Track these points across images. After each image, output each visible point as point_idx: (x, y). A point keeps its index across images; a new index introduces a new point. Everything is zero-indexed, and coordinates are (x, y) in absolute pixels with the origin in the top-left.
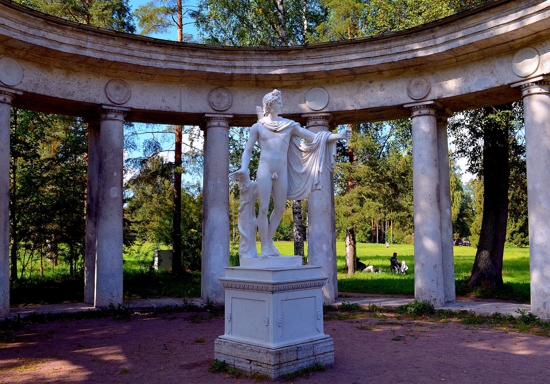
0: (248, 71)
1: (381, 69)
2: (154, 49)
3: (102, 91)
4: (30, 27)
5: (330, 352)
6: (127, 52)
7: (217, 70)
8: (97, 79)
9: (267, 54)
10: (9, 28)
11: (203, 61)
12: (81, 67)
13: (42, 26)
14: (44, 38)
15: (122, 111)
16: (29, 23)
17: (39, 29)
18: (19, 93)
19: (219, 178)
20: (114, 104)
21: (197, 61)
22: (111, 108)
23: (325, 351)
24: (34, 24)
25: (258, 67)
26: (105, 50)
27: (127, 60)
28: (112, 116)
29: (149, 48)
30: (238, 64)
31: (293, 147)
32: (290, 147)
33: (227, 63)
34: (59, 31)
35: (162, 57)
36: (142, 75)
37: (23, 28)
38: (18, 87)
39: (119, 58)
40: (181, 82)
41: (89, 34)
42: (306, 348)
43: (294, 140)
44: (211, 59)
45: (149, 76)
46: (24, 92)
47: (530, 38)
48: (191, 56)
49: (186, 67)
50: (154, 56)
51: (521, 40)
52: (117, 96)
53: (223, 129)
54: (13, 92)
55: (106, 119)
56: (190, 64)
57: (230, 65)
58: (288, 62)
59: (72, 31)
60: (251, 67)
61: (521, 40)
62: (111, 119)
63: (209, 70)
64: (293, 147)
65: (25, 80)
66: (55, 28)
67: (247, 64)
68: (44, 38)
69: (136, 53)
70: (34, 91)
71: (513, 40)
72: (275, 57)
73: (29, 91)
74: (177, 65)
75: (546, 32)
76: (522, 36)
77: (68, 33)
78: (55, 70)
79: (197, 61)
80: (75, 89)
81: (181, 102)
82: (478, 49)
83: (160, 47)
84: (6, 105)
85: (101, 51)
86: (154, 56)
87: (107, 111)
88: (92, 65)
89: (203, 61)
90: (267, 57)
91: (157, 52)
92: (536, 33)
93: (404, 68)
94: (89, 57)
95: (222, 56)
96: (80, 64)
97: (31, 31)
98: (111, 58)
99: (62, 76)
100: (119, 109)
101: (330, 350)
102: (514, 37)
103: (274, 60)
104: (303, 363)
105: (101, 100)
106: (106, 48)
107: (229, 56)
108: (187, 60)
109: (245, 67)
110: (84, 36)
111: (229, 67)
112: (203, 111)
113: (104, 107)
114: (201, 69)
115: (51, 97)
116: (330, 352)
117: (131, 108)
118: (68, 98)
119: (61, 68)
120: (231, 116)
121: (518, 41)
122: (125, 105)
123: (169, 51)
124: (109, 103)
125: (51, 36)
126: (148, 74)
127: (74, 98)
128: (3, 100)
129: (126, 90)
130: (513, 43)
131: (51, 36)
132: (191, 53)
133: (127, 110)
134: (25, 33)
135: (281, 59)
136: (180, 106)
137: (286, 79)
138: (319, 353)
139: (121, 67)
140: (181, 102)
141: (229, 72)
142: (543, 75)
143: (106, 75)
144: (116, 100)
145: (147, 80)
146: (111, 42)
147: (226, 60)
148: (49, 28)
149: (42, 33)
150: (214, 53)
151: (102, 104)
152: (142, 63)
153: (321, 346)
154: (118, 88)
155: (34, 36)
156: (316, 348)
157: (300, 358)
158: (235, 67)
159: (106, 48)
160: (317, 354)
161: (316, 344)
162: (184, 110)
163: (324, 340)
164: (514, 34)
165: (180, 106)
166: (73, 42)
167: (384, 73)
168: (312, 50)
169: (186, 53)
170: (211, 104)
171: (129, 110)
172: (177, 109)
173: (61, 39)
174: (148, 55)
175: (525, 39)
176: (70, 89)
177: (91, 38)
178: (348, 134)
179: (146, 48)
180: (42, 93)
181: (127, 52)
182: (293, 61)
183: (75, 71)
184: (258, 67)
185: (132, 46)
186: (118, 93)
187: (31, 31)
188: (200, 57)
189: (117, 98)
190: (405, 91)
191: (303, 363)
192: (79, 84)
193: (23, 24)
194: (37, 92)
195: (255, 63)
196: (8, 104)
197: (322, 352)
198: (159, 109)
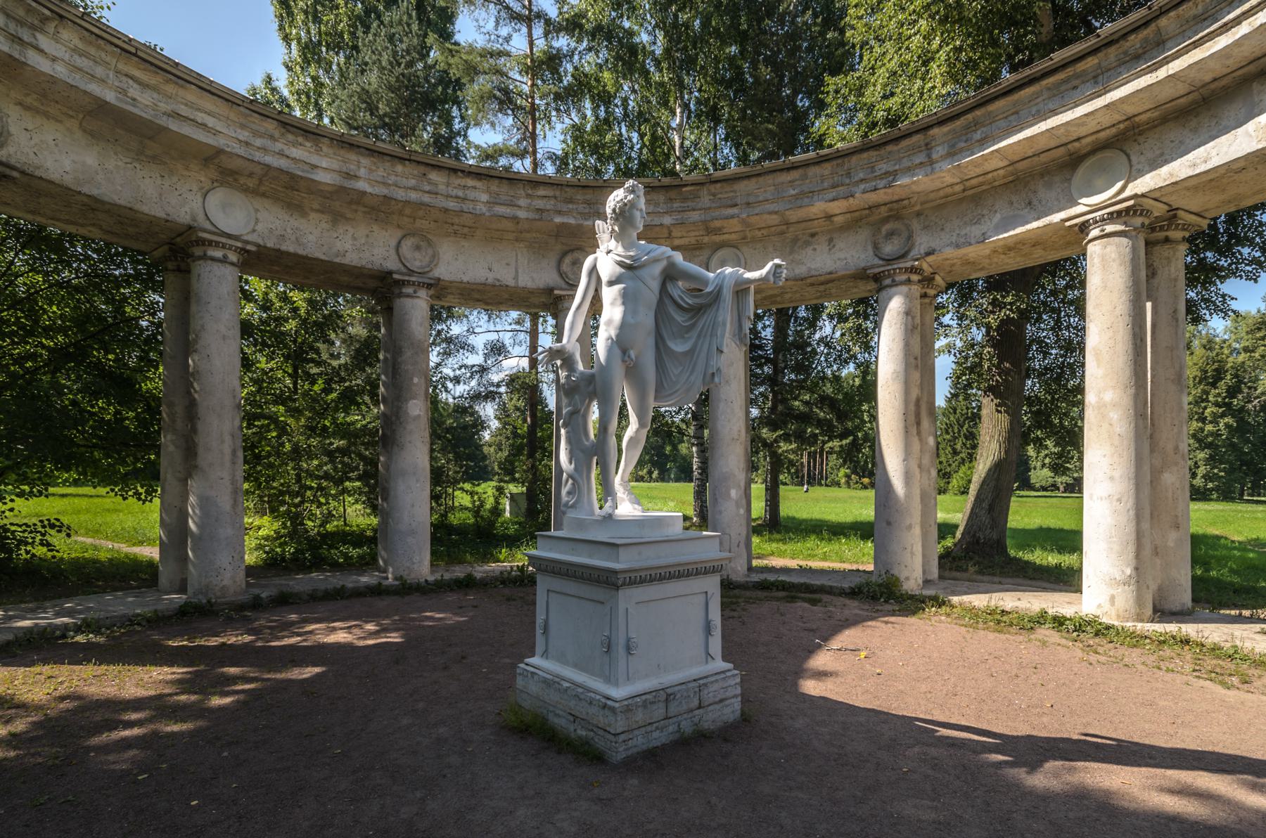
1: (832, 212)
2: (470, 182)
3: (393, 252)
4: (256, 134)
8: (384, 232)
10: (217, 133)
12: (356, 211)
14: (281, 154)
17: (272, 137)
20: (411, 272)
22: (407, 278)
27: (426, 199)
28: (410, 290)
31: (667, 301)
32: (660, 302)
34: (308, 144)
36: (456, 227)
37: (244, 135)
39: (413, 196)
40: (517, 240)
41: (362, 155)
43: (670, 288)
45: (466, 230)
46: (258, 246)
47: (1114, 130)
51: (1093, 137)
52: (417, 261)
55: (400, 295)
61: (1093, 137)
62: (408, 296)
64: (667, 301)
65: (259, 227)
66: (300, 139)
68: (281, 154)
71: (1078, 139)
75: (1149, 115)
76: (1099, 128)
77: (325, 149)
78: (313, 215)
80: (348, 246)
81: (517, 272)
82: (1006, 163)
83: (480, 180)
87: (402, 283)
88: (373, 208)
92: (1129, 119)
93: (870, 208)
94: (364, 193)
96: (354, 207)
98: (400, 194)
99: (324, 225)
102: (1083, 131)
105: (392, 264)
112: (552, 284)
113: (395, 276)
117: (439, 279)
118: (337, 260)
119: (322, 212)
121: (1089, 140)
122: (431, 275)
124: (404, 270)
125: (296, 152)
127: (346, 261)
129: (430, 252)
130: (1076, 144)
131: (296, 152)
132: (530, 192)
134: (247, 144)
136: (516, 278)
137: (679, 234)
139: (421, 213)
140: (517, 272)
142: (1135, 196)
143: (399, 226)
145: (465, 236)
146: (399, 168)
151: (390, 273)
152: (452, 205)
154: (418, 248)
155: (264, 149)
162: (521, 284)
164: (1083, 124)
165: (516, 278)
167: (835, 219)
168: (719, 185)
173: (314, 159)
174: (460, 194)
175: (1102, 135)
176: (339, 245)
179: (459, 181)
181: (427, 188)
182: (690, 204)
183: (347, 219)
186: (417, 255)
189: (417, 263)
190: (870, 248)
192: (354, 239)
193: (243, 127)
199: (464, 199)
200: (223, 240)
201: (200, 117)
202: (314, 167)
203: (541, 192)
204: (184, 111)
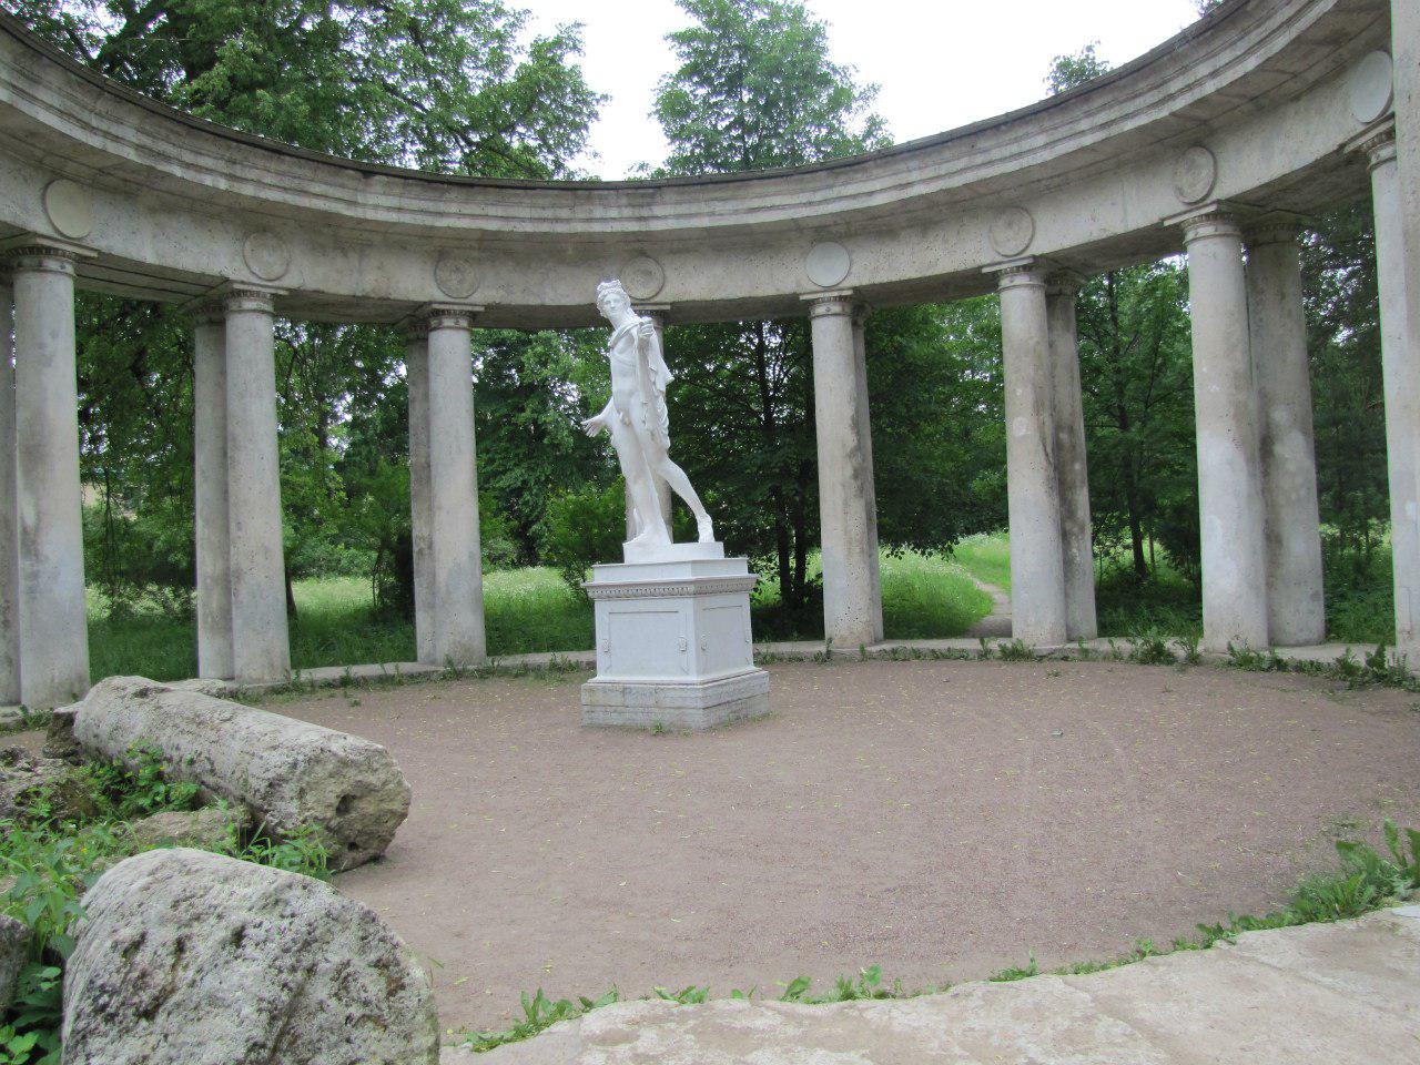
0: (1197, 94)
2: (1020, 132)
4: (814, 191)
6: (979, 159)
7: (1143, 120)
9: (1212, 34)
10: (783, 207)
11: (1113, 114)
13: (831, 181)
15: (1018, 267)
16: (811, 185)
17: (830, 187)
19: (1204, 361)
21: (1102, 118)
24: (819, 184)
25: (1214, 74)
26: (943, 172)
29: (1013, 135)
30: (1174, 87)
33: (1154, 96)
34: (859, 176)
35: (1041, 140)
37: (804, 198)
38: (847, 284)
39: (970, 177)
40: (1118, 167)
44: (1125, 101)
48: (1089, 115)
49: (1088, 140)
50: (1026, 145)
53: (1207, 241)
54: (836, 294)
56: (1093, 130)
57: (1161, 96)
58: (1260, 30)
59: (877, 167)
60: (1199, 83)
63: (1129, 125)
67: (1190, 78)
69: (996, 154)
70: (872, 282)
72: (1233, 34)
74: (1072, 143)
79: (1102, 118)
81: (1125, 211)
83: (1027, 123)
85: (939, 177)
86: (1026, 145)
89: (1113, 114)
90: (1218, 42)
91: (1027, 136)
95: (1142, 85)
97: (818, 197)
100: (1013, 265)
103: (1234, 43)
106: (943, 169)
107: (1152, 80)
108: (1084, 125)
109: (1189, 87)
110: (902, 166)
111: (1162, 102)
113: (985, 270)
114: (1115, 130)
115: (901, 282)
117: (1034, 257)
118: (929, 273)
120: (1212, 208)
123: (1047, 124)
125: (852, 189)
126: (1052, 177)
132: (1085, 108)
133: (1025, 262)
134: (810, 204)
135: (1246, 33)
141: (1163, 113)
144: (1011, 247)
147: (1150, 90)
148: (843, 178)
149: (834, 193)
150: (1125, 87)
153: (672, 694)
154: (1010, 225)
155: (826, 201)
158: (1171, 97)
159: (943, 169)
166: (889, 182)
169: (1078, 113)
170: (1180, 191)
171: (1031, 261)
172: (1119, 229)
173: (869, 187)
174: (1014, 149)
177: (913, 164)
181: (979, 159)
183: (936, 223)
184: (1214, 74)
185: (982, 143)
187: (818, 197)
188: (1103, 107)
191: (636, 713)
193: (803, 191)
194: (878, 280)
195: (1203, 70)
196: (835, 315)
198: (1087, 241)
199: (1020, 155)
200: (821, 295)
201: (768, 202)
202: (871, 194)
203: (1098, 102)
204: (756, 203)
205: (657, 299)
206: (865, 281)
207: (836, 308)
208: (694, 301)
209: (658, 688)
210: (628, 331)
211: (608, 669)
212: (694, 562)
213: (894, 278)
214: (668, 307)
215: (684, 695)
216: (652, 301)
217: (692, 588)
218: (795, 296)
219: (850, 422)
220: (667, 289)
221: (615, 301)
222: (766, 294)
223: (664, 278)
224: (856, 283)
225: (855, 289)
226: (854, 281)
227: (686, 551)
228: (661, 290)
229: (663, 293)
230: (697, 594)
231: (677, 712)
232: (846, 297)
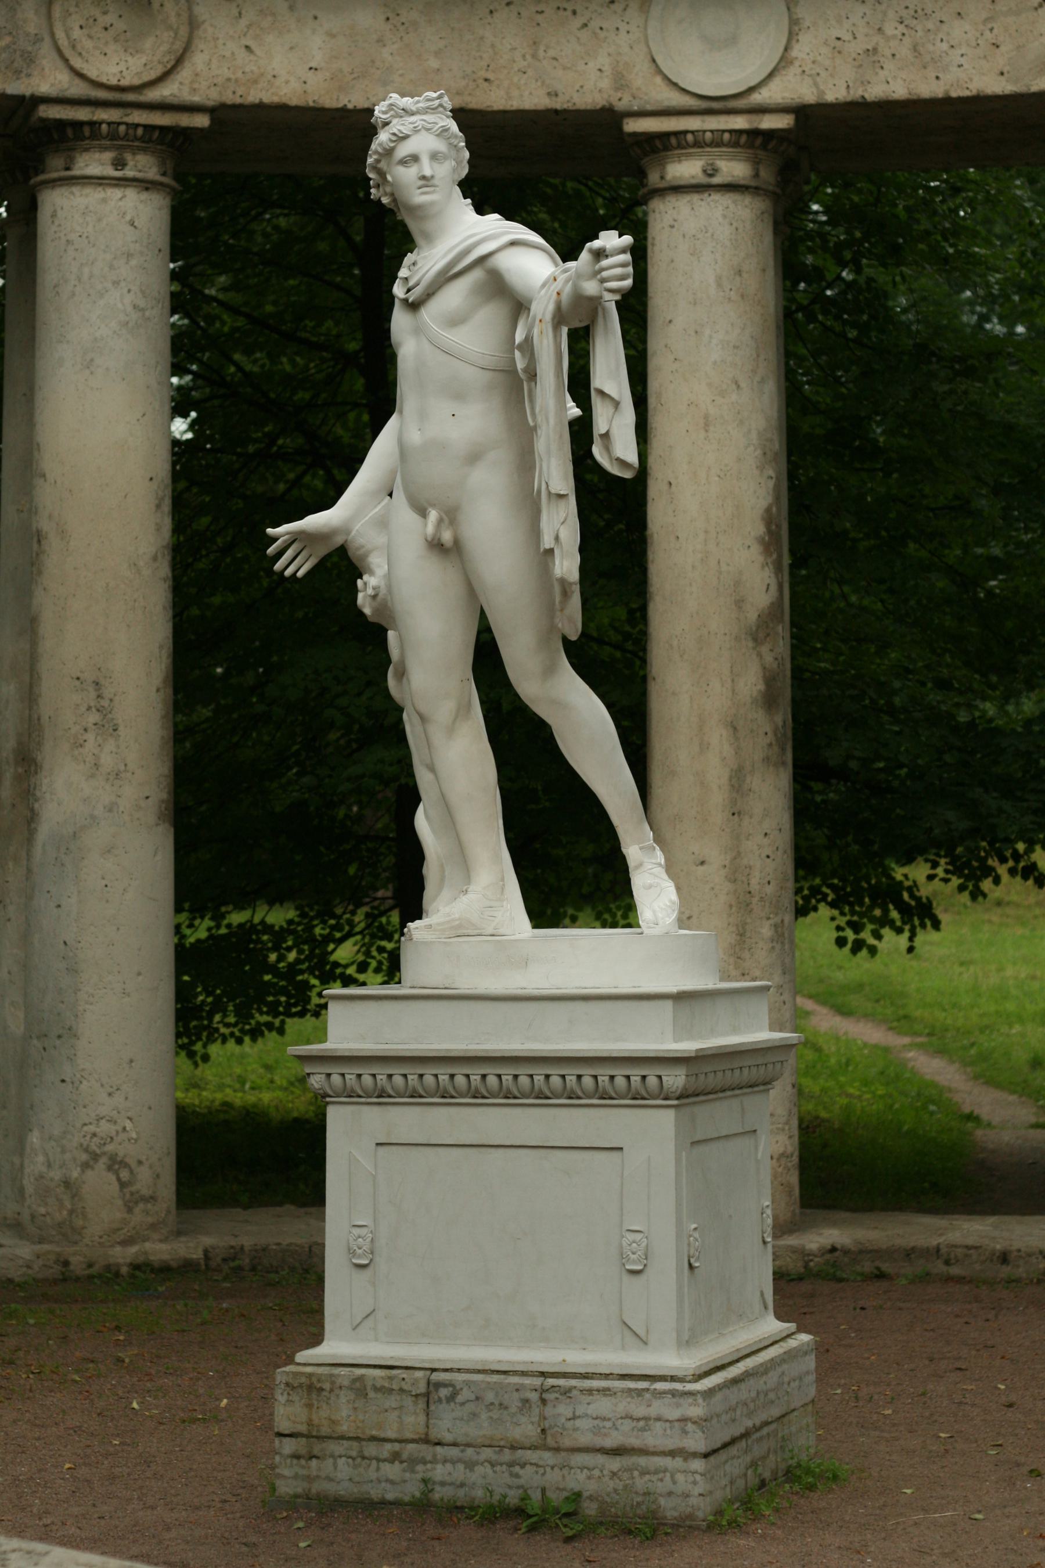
5: (672, 1454)
18: (768, 123)
23: (634, 1442)
38: (773, 94)
42: (490, 1397)
54: (740, 123)
70: (857, 93)
73: (830, 97)
84: (716, 197)
101: (671, 1444)
104: (470, 1465)
115: (947, 101)
116: (672, 1454)
128: (703, 179)
138: (585, 1439)
153: (602, 1406)
156: (564, 1410)
157: (448, 1437)
160: (567, 1442)
161: (566, 1392)
163: (632, 1385)
178: (605, 263)
180: (899, 91)
191: (470, 1465)
194: (876, 91)
197: (608, 1443)
205: (165, 92)
206: (835, 93)
207: (734, 168)
208: (283, 108)
209: (550, 1386)
210: (482, 259)
211: (364, 1321)
212: (680, 997)
213: (929, 88)
214: (202, 121)
215: (640, 1411)
216: (153, 95)
217: (675, 1079)
218: (609, 118)
219: (761, 529)
220: (198, 60)
221: (434, 156)
222: (515, 104)
223: (193, 24)
224: (808, 95)
225: (802, 112)
226: (793, 88)
227: (582, 956)
228: (179, 61)
229: (185, 73)
230: (685, 1097)
231: (615, 1464)
232: (769, 135)
